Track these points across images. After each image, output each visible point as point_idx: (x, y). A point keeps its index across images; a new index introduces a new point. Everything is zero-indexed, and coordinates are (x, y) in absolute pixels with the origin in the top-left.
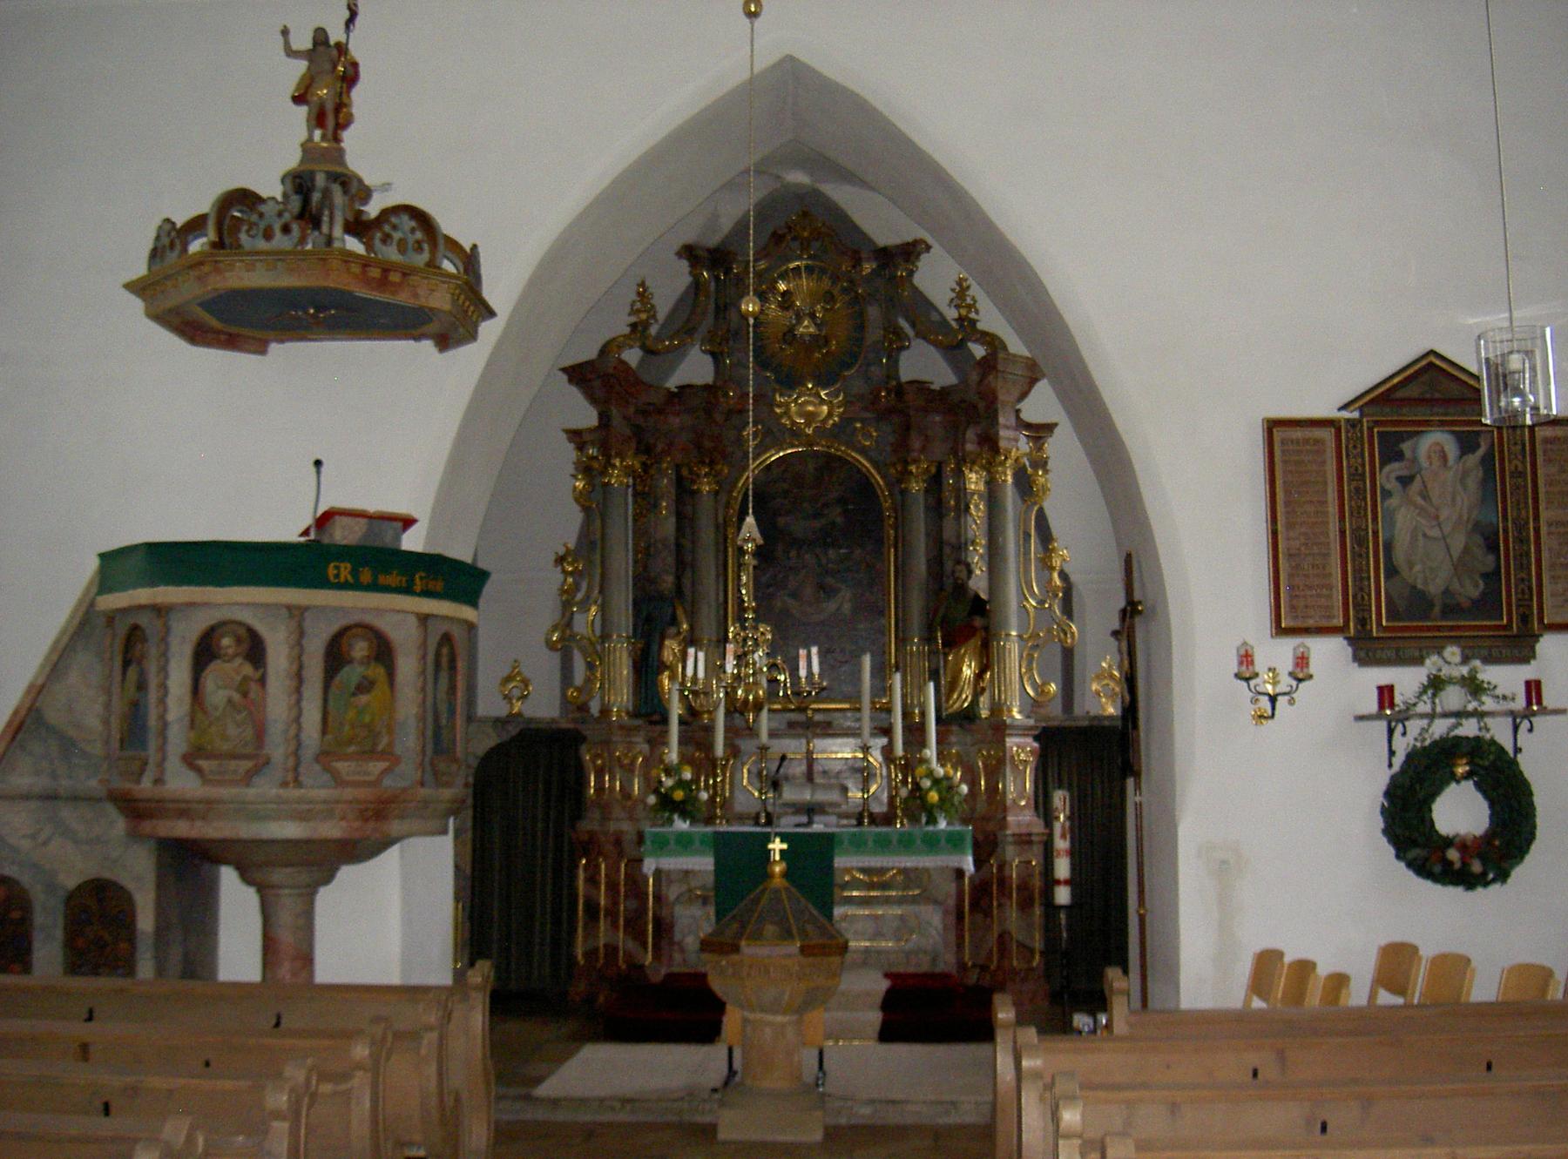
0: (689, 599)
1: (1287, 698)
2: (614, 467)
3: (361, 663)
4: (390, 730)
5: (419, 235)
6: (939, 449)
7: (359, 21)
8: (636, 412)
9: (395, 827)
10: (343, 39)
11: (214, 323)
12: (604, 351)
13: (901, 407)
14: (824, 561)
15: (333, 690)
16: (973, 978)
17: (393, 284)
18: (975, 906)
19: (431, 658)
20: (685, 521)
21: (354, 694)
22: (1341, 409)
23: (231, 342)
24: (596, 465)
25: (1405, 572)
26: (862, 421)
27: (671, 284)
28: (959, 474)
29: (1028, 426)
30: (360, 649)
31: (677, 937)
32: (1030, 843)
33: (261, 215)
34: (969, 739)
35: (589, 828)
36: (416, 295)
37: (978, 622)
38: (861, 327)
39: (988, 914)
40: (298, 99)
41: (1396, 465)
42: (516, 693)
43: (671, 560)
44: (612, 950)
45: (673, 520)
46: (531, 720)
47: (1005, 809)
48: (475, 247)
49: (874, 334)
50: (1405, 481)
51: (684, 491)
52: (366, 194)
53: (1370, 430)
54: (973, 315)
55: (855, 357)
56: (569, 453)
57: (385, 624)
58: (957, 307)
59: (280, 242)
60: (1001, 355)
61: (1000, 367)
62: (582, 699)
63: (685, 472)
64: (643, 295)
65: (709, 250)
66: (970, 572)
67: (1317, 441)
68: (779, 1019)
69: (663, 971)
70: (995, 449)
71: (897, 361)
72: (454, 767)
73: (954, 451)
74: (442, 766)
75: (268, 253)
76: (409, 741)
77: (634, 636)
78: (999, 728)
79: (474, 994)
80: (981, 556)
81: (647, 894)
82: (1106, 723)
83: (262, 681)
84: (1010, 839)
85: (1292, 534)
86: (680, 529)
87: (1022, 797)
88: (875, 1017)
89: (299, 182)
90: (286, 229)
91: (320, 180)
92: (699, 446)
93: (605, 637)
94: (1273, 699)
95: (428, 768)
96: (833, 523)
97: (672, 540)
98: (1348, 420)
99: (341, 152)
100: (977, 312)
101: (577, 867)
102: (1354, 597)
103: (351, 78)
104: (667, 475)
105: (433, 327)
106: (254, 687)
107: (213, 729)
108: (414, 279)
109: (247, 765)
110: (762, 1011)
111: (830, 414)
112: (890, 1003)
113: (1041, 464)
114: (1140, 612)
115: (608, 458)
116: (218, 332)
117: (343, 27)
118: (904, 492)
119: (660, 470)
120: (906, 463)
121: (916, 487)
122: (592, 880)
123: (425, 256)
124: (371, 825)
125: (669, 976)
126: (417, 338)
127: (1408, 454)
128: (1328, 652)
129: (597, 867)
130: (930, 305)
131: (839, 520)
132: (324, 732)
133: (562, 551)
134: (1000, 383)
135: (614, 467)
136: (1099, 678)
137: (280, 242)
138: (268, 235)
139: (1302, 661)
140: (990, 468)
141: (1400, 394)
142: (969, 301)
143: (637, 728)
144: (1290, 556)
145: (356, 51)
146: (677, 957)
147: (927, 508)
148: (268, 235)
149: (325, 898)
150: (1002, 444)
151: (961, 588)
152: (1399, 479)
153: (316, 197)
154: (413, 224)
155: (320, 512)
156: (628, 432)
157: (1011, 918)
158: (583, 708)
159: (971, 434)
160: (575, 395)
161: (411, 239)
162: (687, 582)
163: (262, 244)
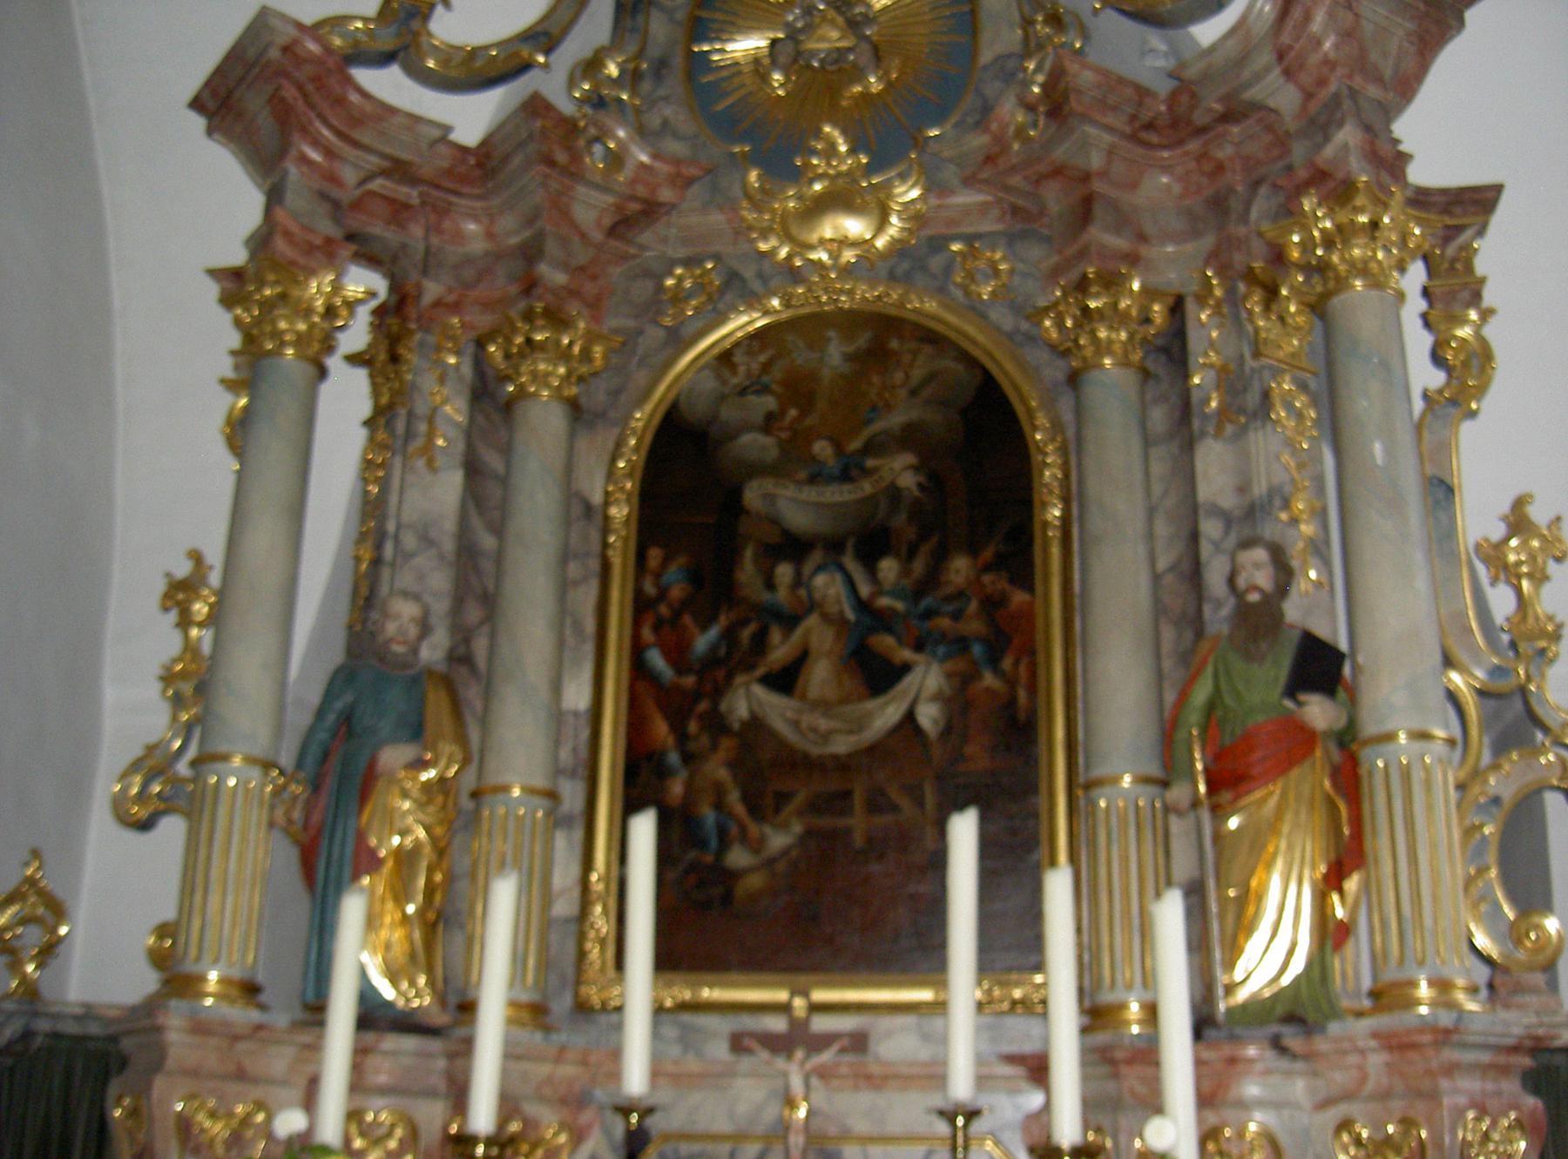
6: (1175, 261)
14: (865, 590)
34: (1299, 1088)
37: (1318, 712)
43: (440, 581)
51: (492, 400)
92: (530, 286)
96: (895, 493)
97: (450, 525)
131: (908, 481)
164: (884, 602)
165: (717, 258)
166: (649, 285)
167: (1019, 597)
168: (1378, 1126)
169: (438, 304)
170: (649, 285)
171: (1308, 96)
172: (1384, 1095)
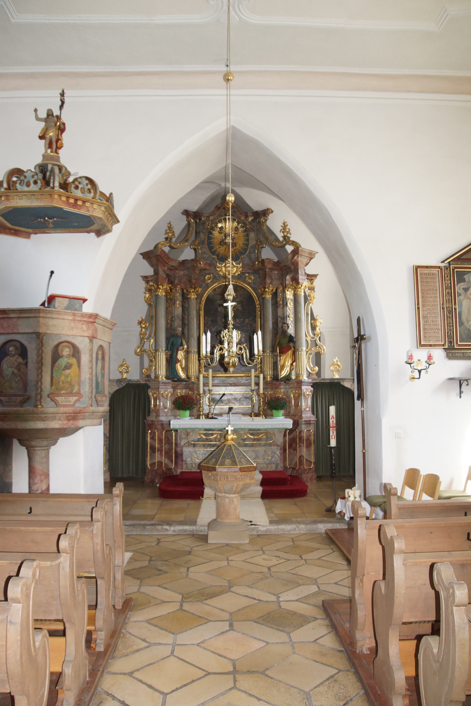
0: (187, 337)
1: (425, 371)
2: (160, 289)
3: (66, 357)
4: (79, 385)
5: (89, 186)
6: (276, 283)
7: (65, 106)
8: (168, 269)
9: (80, 423)
10: (59, 114)
11: (9, 225)
12: (156, 247)
13: (259, 270)
15: (55, 368)
16: (289, 472)
17: (79, 205)
18: (290, 446)
19: (94, 355)
20: (185, 310)
21: (64, 370)
22: (443, 262)
23: (16, 233)
24: (153, 288)
25: (466, 324)
26: (248, 273)
27: (180, 224)
28: (284, 292)
29: (308, 275)
30: (66, 351)
31: (184, 459)
32: (310, 424)
33: (25, 177)
34: (287, 387)
35: (151, 419)
36: (88, 211)
37: (291, 344)
38: (248, 240)
39: (295, 449)
40: (42, 137)
41: (462, 284)
42: (124, 371)
43: (180, 323)
44: (160, 463)
45: (181, 308)
46: (130, 380)
47: (302, 412)
48: (111, 194)
49: (252, 242)
50: (466, 290)
51: (185, 298)
52: (69, 174)
53: (453, 270)
54: (289, 235)
55: (245, 250)
56: (143, 284)
57: (76, 341)
58: (283, 232)
59: (33, 187)
60: (300, 249)
61: (300, 253)
62: (148, 373)
63: (185, 291)
64: (170, 228)
65: (193, 212)
66: (288, 327)
67: (433, 274)
68: (231, 496)
69: (179, 471)
70: (298, 283)
71: (261, 252)
72: (104, 398)
73: (282, 284)
74: (99, 398)
75: (28, 192)
76: (86, 389)
77: (167, 349)
78: (299, 383)
79: (115, 498)
80: (292, 322)
81: (172, 443)
82: (336, 381)
83: (26, 364)
84: (304, 422)
85: (424, 309)
86: (183, 311)
87: (307, 408)
88: (260, 489)
89: (42, 168)
90: (35, 182)
91: (50, 167)
92: (190, 281)
93: (156, 350)
94: (420, 372)
95: (94, 399)
97: (181, 315)
98: (444, 267)
99: (59, 158)
100: (290, 234)
101: (147, 433)
102: (448, 333)
103: (62, 129)
104: (178, 292)
105: (95, 227)
106: (23, 366)
107: (7, 384)
108: (88, 204)
109: (20, 399)
110: (225, 493)
111: (237, 271)
112: (263, 483)
113: (312, 289)
114: (365, 339)
115: (158, 285)
116: (10, 229)
117: (58, 108)
118: (263, 299)
119: (176, 290)
120: (265, 288)
121: (268, 296)
122: (153, 438)
123: (92, 194)
124: (71, 422)
125: (181, 472)
126: (88, 232)
127: (467, 280)
128: (439, 354)
129: (155, 433)
130: (272, 233)
132: (52, 385)
133: (140, 320)
134: (299, 258)
135: (160, 289)
136: (333, 364)
137: (33, 187)
138: (28, 185)
139: (430, 357)
140: (295, 289)
141: (464, 257)
142: (287, 230)
143: (169, 383)
144: (424, 317)
145: (64, 119)
146: (184, 466)
147: (272, 305)
148: (28, 185)
149: (54, 450)
150: (300, 281)
151: (284, 332)
152: (463, 289)
153: (48, 174)
154: (87, 182)
155: (49, 294)
156: (165, 276)
157: (304, 451)
158: (149, 376)
159: (288, 277)
160: (145, 263)
161: (86, 188)
162: (186, 332)
163: (25, 188)
164: (237, 325)
165: (212, 274)
166: (203, 277)
167: (254, 325)
168: (295, 391)
169: (177, 283)
170: (203, 277)
171: (295, 267)
172: (296, 388)
